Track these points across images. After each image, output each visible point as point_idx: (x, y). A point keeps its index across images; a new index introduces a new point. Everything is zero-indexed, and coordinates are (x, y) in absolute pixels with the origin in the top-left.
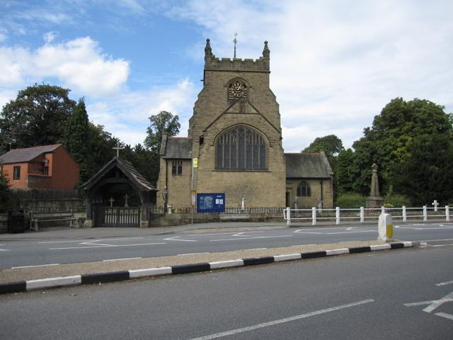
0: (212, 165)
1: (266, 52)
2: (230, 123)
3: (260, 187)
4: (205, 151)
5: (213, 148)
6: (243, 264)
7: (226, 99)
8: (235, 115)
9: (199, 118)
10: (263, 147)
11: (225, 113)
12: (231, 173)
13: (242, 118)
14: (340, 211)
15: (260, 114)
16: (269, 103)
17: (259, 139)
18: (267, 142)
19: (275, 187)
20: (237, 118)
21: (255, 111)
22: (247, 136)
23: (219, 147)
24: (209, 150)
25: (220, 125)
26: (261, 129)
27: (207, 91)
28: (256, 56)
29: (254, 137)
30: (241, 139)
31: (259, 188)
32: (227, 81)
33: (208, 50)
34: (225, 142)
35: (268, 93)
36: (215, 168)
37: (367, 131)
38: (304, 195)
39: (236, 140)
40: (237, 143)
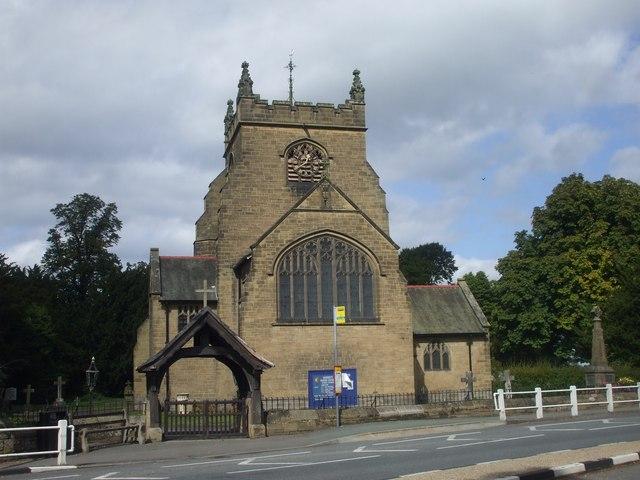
0: (270, 312)
1: (357, 91)
2: (304, 231)
3: (365, 354)
4: (256, 286)
6: (584, 470)
7: (282, 181)
9: (230, 217)
10: (367, 276)
11: (294, 210)
13: (326, 220)
14: (544, 395)
15: (359, 212)
16: (365, 189)
17: (360, 260)
18: (375, 266)
19: (393, 354)
21: (350, 207)
22: (338, 255)
23: (283, 277)
24: (263, 286)
25: (286, 235)
26: (363, 241)
28: (339, 97)
29: (351, 257)
30: (324, 260)
31: (362, 357)
32: (284, 145)
33: (245, 83)
34: (295, 267)
35: (364, 169)
37: (521, 237)
38: (437, 367)
39: (317, 263)
40: (318, 270)
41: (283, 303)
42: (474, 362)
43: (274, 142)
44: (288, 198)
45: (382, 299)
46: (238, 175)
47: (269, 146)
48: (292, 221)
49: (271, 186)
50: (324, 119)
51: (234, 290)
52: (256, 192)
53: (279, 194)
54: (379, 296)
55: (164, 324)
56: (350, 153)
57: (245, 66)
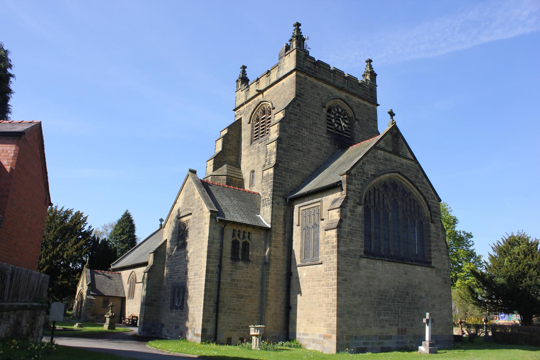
3: (423, 294)
4: (349, 214)
5: (360, 209)
8: (388, 155)
20: (390, 160)
21: (411, 157)
27: (299, 105)
31: (421, 297)
36: (366, 252)
43: (318, 94)
44: (327, 144)
46: (292, 113)
47: (315, 96)
48: (375, 157)
49: (316, 131)
50: (352, 88)
51: (284, 220)
53: (322, 139)
54: (430, 241)
56: (368, 120)
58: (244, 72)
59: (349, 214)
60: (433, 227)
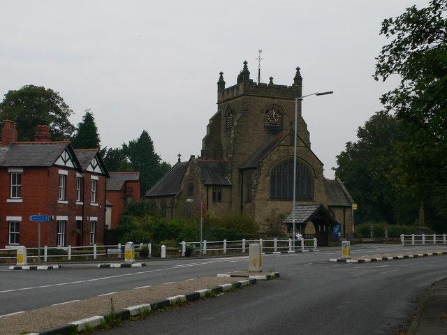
0: (267, 194)
1: (298, 79)
4: (261, 181)
12: (283, 203)
21: (303, 144)
23: (273, 180)
26: (309, 161)
27: (246, 116)
28: (289, 82)
41: (272, 190)
42: (346, 220)
43: (259, 105)
45: (315, 189)
52: (250, 130)
54: (313, 188)
55: (206, 196)
57: (245, 63)
58: (221, 77)
59: (261, 181)
60: (316, 181)
